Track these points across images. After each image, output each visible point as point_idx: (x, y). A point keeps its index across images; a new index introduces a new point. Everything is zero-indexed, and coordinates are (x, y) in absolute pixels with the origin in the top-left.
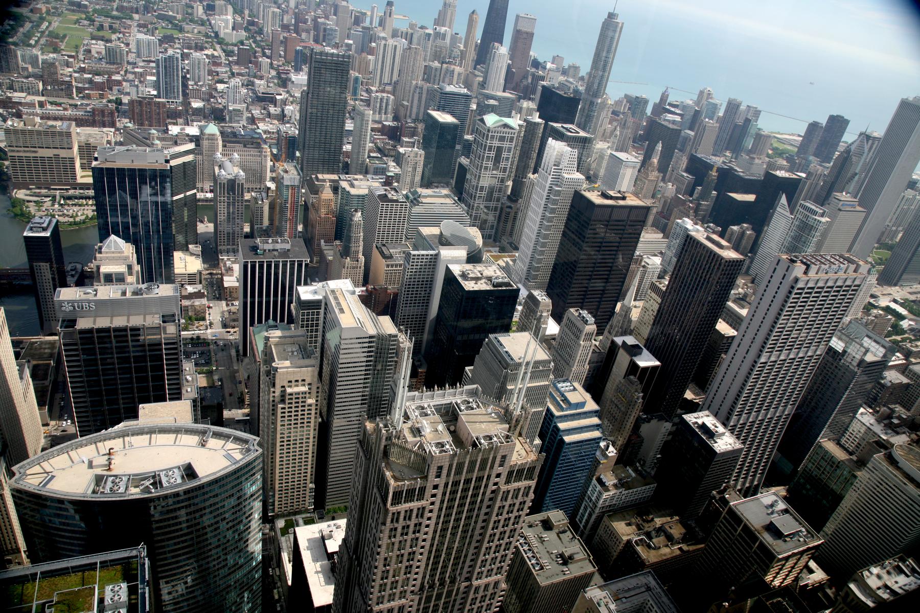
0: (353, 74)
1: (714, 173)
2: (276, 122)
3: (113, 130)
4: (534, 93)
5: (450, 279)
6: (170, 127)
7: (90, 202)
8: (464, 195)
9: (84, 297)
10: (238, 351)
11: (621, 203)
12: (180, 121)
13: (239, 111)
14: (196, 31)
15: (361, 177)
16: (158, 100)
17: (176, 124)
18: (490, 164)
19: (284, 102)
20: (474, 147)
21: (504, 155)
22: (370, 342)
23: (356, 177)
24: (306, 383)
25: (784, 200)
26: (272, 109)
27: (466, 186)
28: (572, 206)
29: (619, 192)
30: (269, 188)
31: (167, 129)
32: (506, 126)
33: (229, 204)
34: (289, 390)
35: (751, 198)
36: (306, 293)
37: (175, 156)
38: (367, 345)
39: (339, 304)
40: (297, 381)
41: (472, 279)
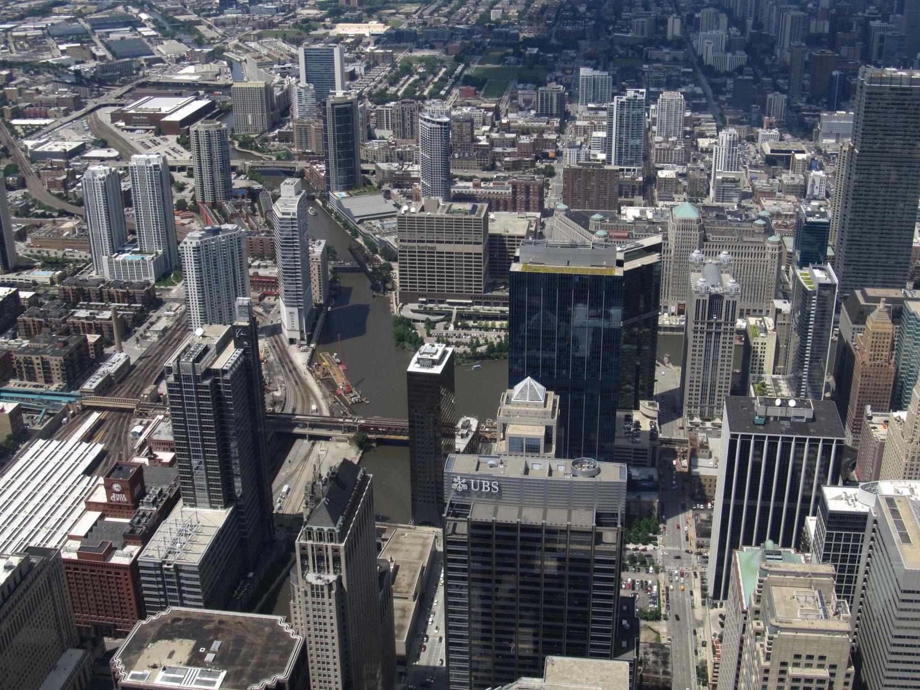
2: (792, 198)
3: (538, 215)
6: (624, 209)
7: (498, 324)
9: (483, 470)
10: (704, 589)
12: (639, 199)
13: (734, 181)
14: (667, 58)
16: (607, 167)
17: (631, 204)
19: (810, 165)
24: (827, 663)
26: (787, 177)
30: (779, 311)
31: (619, 212)
33: (709, 333)
34: (792, 671)
36: (838, 498)
37: (630, 256)
39: (900, 525)
40: (810, 657)
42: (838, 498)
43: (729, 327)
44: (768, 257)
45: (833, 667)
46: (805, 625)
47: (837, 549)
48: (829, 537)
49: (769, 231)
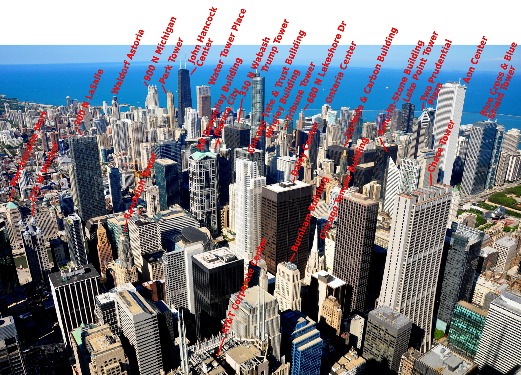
0: (101, 149)
1: (344, 154)
2: (56, 191)
4: (220, 132)
5: (196, 266)
8: (192, 208)
11: (293, 188)
15: (121, 213)
18: (204, 184)
20: (190, 175)
21: (211, 176)
22: (154, 321)
23: (118, 213)
25: (391, 160)
27: (191, 202)
28: (262, 197)
29: (290, 181)
32: (207, 158)
35: (372, 164)
38: (152, 323)
40: (110, 360)
41: (211, 261)
42: (102, 299)
43: (43, 247)
44: (52, 216)
45: (120, 360)
46: (105, 349)
47: (108, 317)
48: (104, 314)
49: (49, 205)
